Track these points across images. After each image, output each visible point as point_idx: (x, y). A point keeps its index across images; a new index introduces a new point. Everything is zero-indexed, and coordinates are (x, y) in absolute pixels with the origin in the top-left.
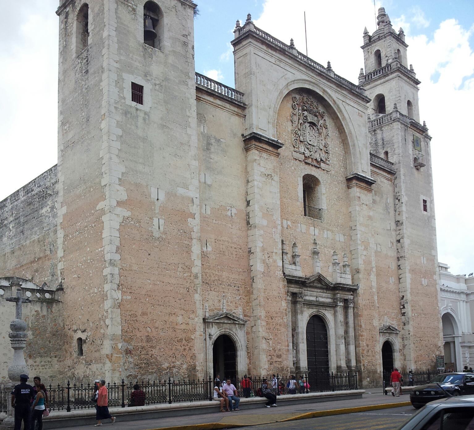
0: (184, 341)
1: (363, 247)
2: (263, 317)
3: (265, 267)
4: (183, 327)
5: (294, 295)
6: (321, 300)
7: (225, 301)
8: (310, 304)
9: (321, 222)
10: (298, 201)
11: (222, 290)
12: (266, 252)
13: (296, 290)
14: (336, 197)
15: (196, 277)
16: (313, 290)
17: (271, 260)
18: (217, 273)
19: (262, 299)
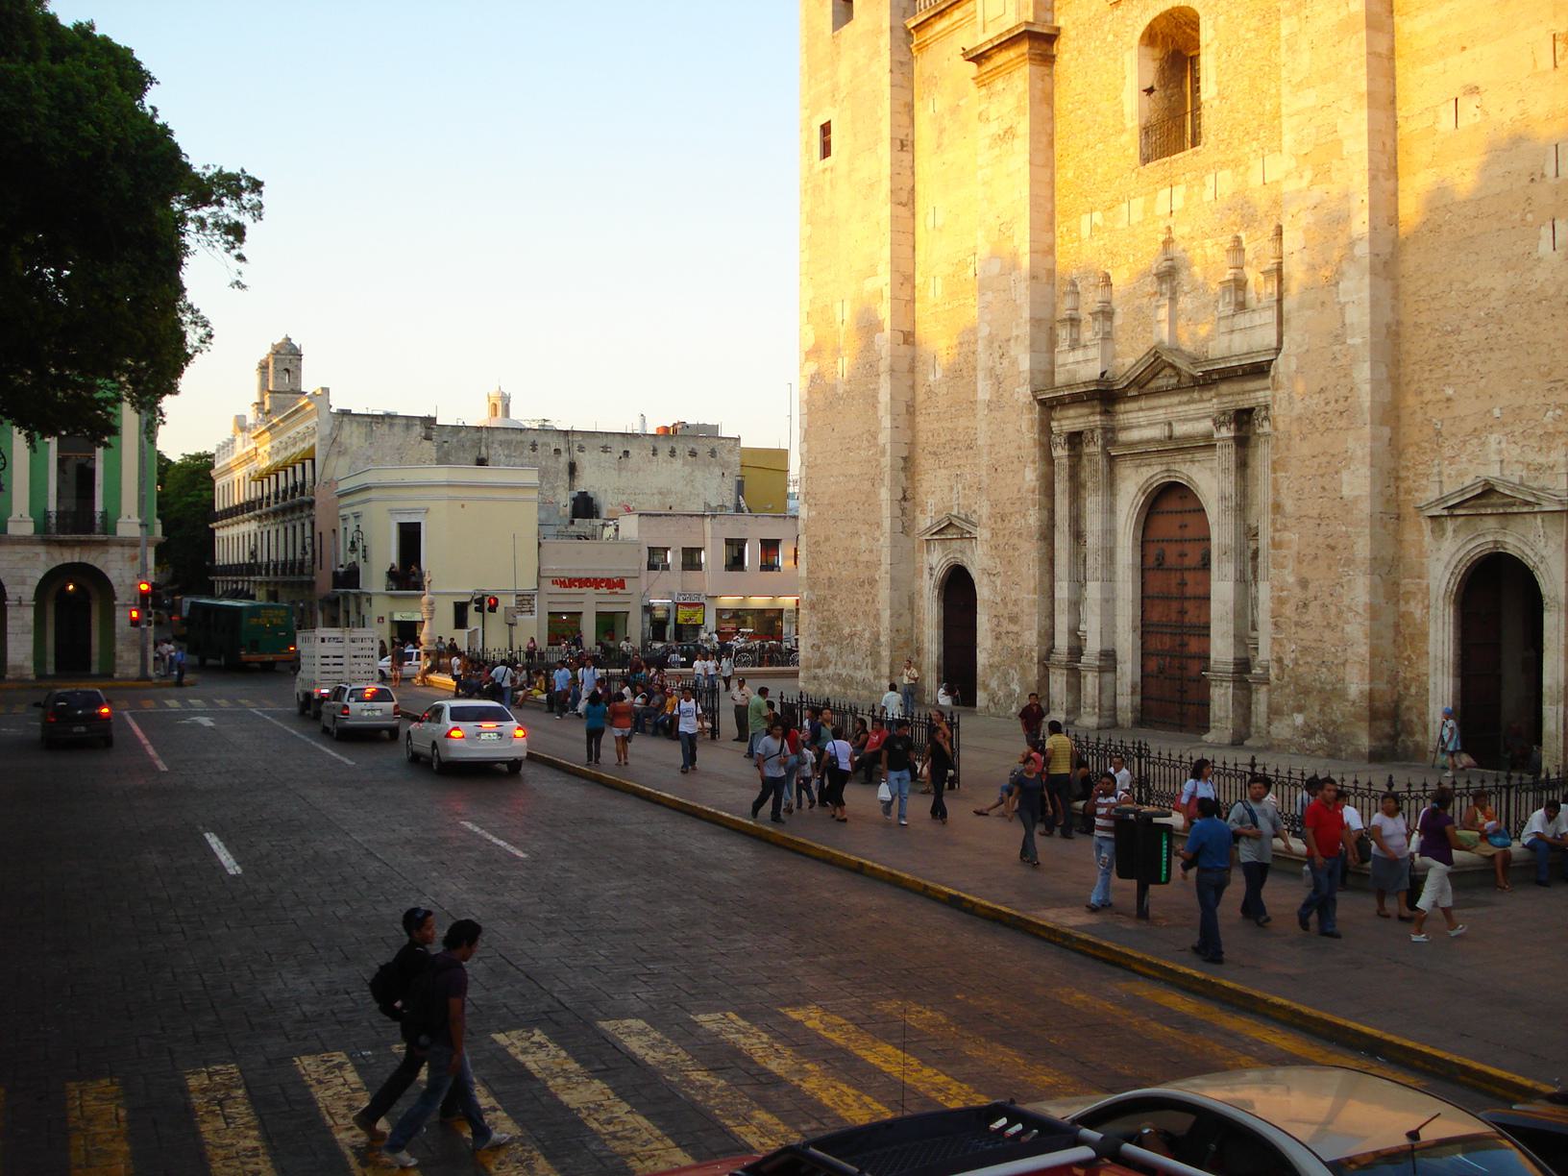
0: (866, 586)
1: (1308, 175)
2: (984, 520)
3: (993, 384)
4: (865, 557)
5: (1075, 439)
6: (1180, 430)
7: (960, 486)
8: (1142, 453)
9: (1196, 153)
10: (1124, 130)
11: (956, 463)
12: (996, 345)
13: (1078, 425)
14: (1254, 23)
15: (883, 453)
16: (1155, 402)
17: (1006, 362)
18: (951, 426)
19: (984, 473)
